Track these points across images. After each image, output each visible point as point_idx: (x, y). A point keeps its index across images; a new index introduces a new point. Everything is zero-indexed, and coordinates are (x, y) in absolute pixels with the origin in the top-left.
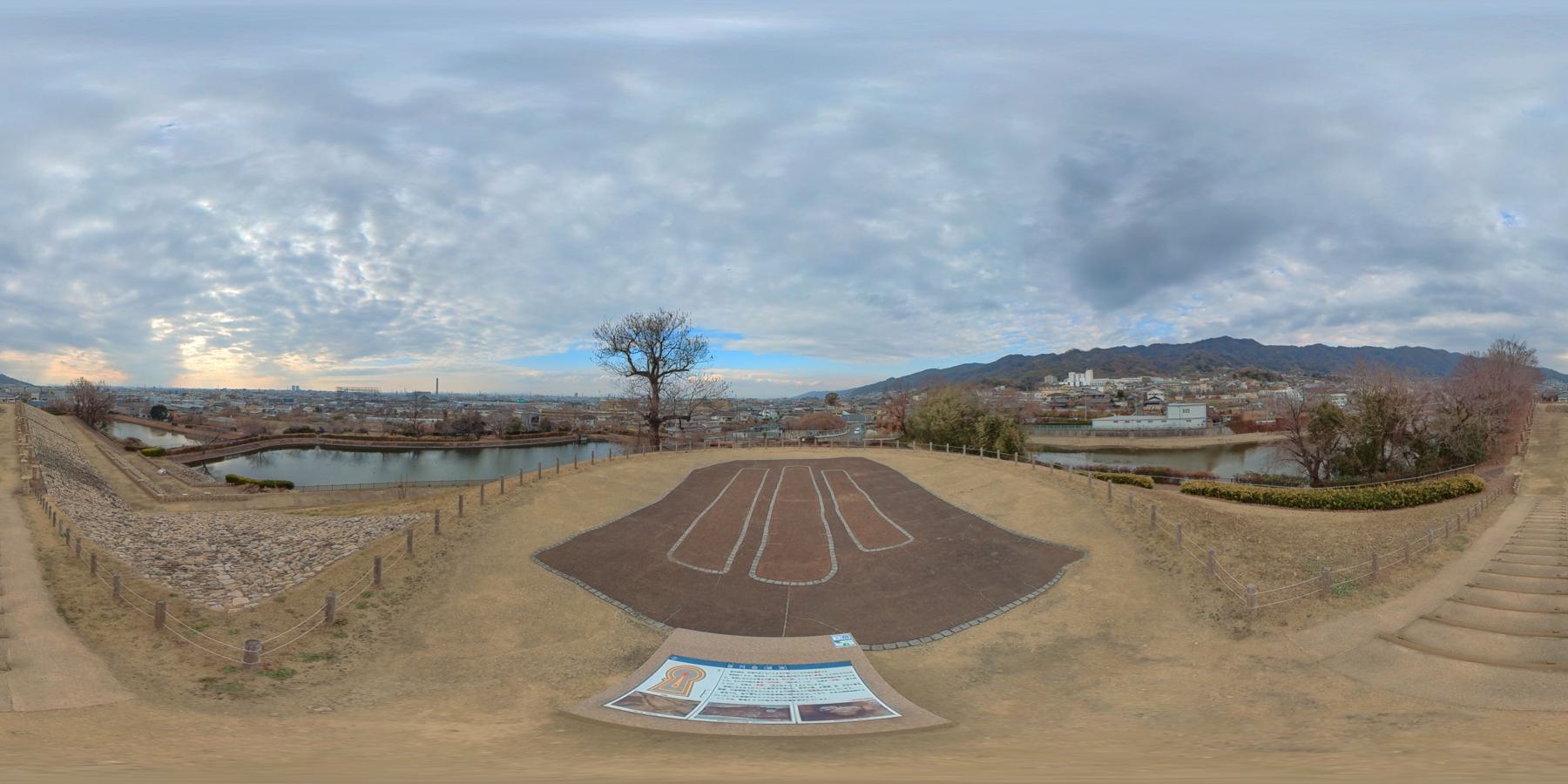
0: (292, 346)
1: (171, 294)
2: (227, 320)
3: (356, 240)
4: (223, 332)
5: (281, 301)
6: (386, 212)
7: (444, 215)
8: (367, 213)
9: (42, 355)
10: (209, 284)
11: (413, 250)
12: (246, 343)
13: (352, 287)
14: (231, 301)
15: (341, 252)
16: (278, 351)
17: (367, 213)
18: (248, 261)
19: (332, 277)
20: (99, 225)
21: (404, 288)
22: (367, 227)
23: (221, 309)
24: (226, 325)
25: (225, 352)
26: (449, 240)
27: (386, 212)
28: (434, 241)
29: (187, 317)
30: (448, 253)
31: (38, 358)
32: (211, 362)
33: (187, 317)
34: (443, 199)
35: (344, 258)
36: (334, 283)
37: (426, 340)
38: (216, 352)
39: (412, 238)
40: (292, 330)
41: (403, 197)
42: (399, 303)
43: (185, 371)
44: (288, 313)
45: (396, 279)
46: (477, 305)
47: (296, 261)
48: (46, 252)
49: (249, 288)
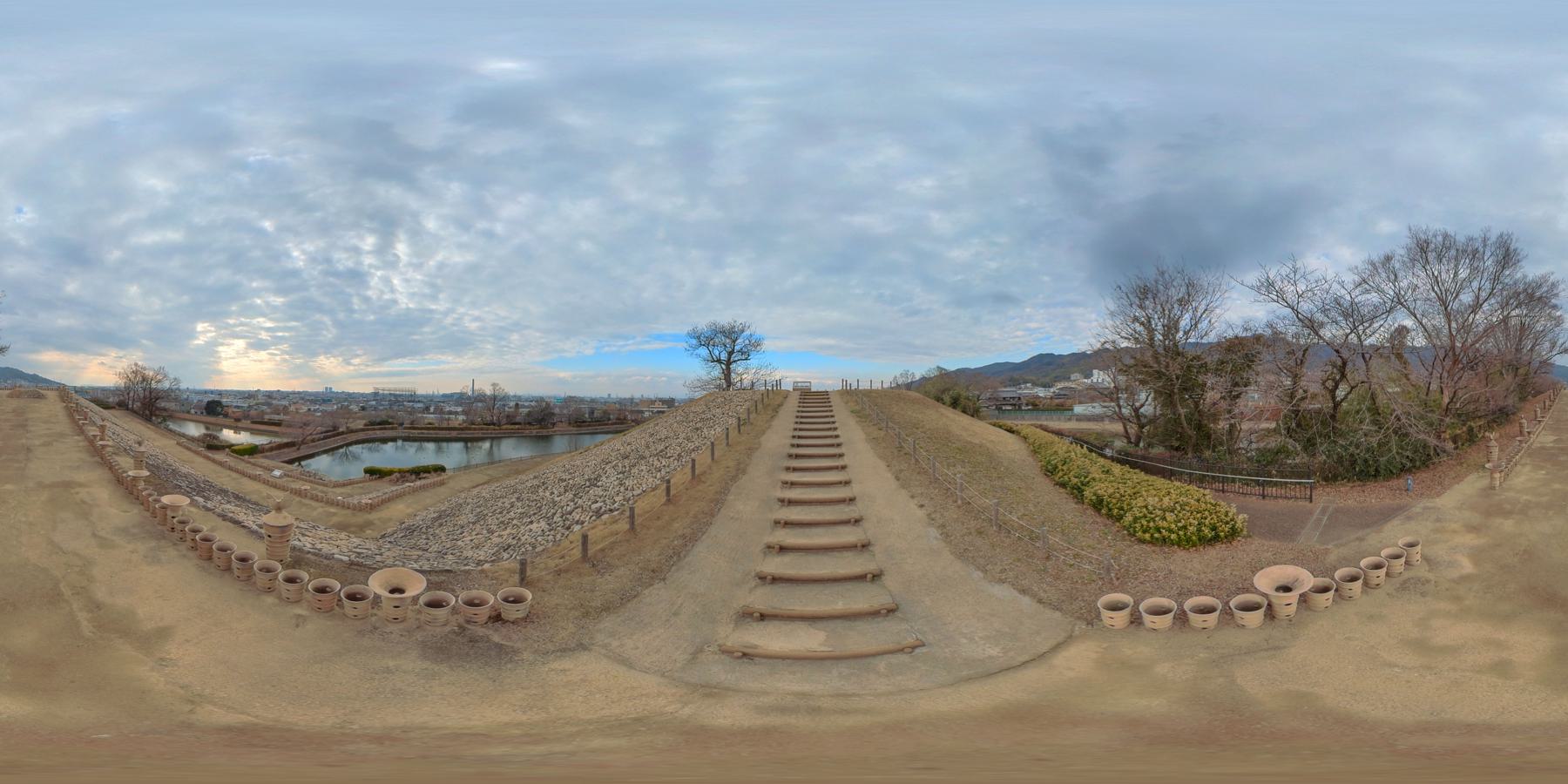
0: (328, 349)
1: (217, 302)
2: (269, 324)
3: (391, 258)
4: (264, 335)
5: (320, 308)
6: (416, 234)
7: (465, 238)
9: (82, 356)
10: (257, 292)
12: (285, 347)
13: (387, 297)
14: (275, 309)
15: (378, 268)
16: (315, 354)
17: (402, 236)
18: (295, 273)
19: (368, 288)
20: (173, 236)
21: (434, 298)
22: (402, 249)
23: (263, 315)
24: (268, 330)
25: (263, 355)
26: (470, 258)
27: (416, 234)
28: (459, 258)
29: (231, 321)
30: (473, 269)
31: (76, 359)
32: (244, 363)
33: (231, 321)
34: (464, 225)
35: (379, 273)
36: (369, 293)
37: (458, 342)
38: (254, 355)
39: (439, 257)
40: (330, 334)
41: (431, 224)
42: (431, 311)
43: (220, 373)
44: (327, 319)
45: (427, 291)
46: (502, 313)
47: (337, 274)
48: (115, 255)
49: (294, 297)
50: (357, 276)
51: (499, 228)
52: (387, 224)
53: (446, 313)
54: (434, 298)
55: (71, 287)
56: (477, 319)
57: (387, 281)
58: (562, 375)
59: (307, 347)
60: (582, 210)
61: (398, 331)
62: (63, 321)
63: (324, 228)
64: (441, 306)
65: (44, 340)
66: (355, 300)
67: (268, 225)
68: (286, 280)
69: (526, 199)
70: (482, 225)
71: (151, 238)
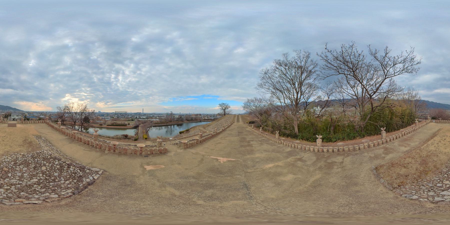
0: (101, 100)
2: (86, 94)
4: (84, 97)
6: (124, 74)
7: (135, 76)
8: (121, 75)
11: (130, 81)
13: (116, 88)
14: (88, 91)
16: (97, 102)
17: (121, 75)
18: (94, 82)
20: (67, 73)
22: (120, 78)
24: (85, 96)
26: (137, 79)
30: (138, 82)
31: (30, 104)
34: (135, 73)
41: (127, 72)
44: (101, 93)
50: (109, 83)
51: (143, 73)
52: (117, 73)
53: (132, 92)
54: (128, 88)
55: (36, 84)
56: (140, 93)
57: (116, 85)
58: (165, 107)
59: (95, 100)
60: (160, 68)
61: (120, 96)
62: (29, 93)
63: (103, 73)
64: (130, 90)
66: (108, 88)
67: (90, 71)
68: (91, 84)
69: (148, 66)
70: (138, 72)
71: (62, 73)
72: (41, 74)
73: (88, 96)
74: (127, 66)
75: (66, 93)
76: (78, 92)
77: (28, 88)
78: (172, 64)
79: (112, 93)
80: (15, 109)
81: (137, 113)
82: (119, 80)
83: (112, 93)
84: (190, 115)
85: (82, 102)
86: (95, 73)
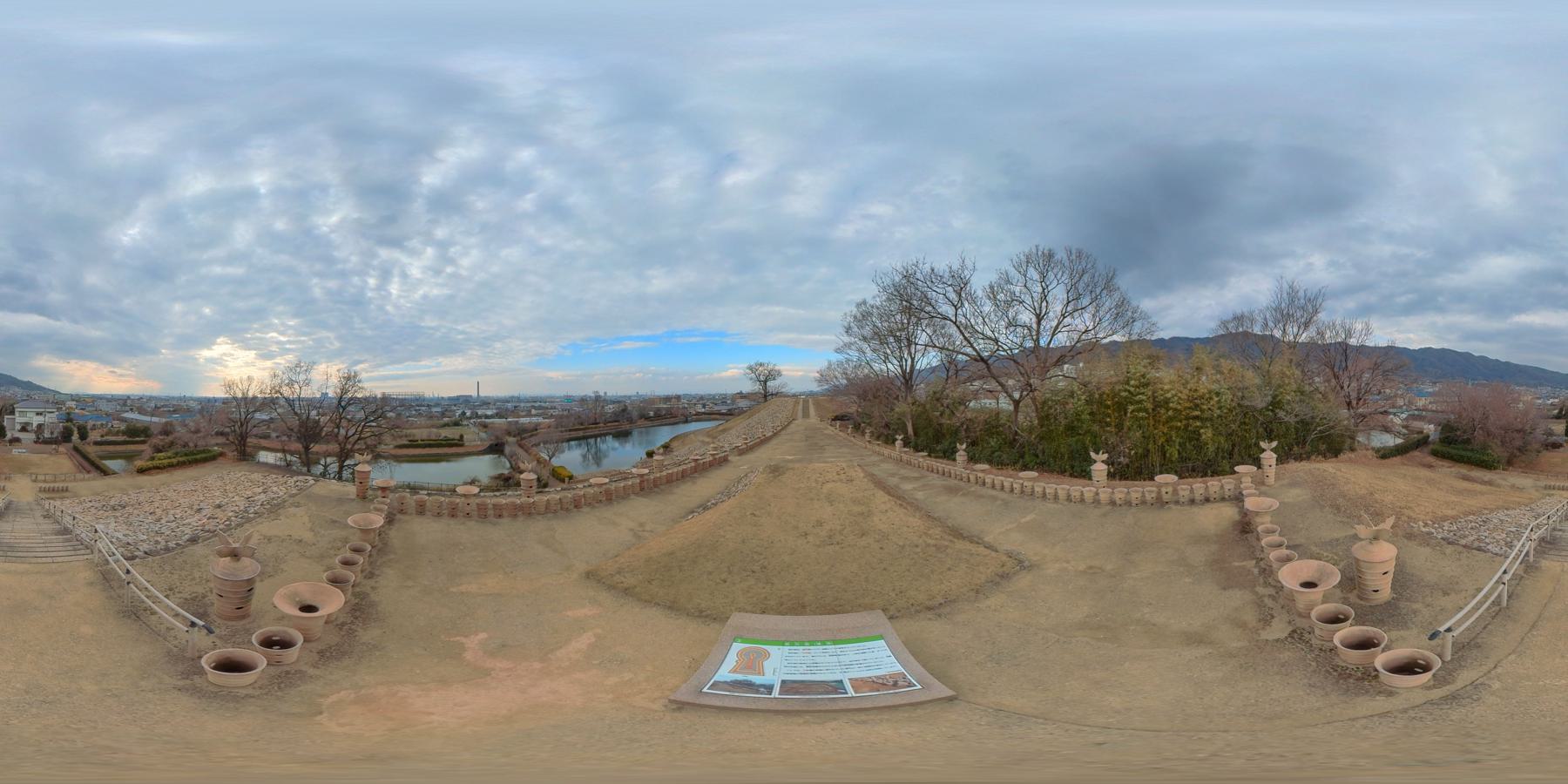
2: (282, 339)
4: (274, 348)
6: (404, 276)
7: (440, 280)
11: (425, 297)
14: (291, 327)
20: (237, 271)
22: (394, 288)
24: (279, 343)
26: (446, 291)
34: (438, 272)
44: (331, 335)
50: (358, 302)
51: (464, 273)
55: (127, 302)
57: (381, 308)
62: (93, 332)
65: (71, 349)
68: (304, 307)
70: (449, 270)
71: (218, 270)
72: (154, 270)
73: (289, 342)
74: (413, 253)
75: (218, 335)
76: (257, 331)
77: (94, 316)
78: (546, 242)
79: (370, 333)
80: (29, 386)
81: (458, 398)
82: (390, 294)
83: (370, 333)
84: (650, 401)
85: (269, 364)
86: (320, 275)
